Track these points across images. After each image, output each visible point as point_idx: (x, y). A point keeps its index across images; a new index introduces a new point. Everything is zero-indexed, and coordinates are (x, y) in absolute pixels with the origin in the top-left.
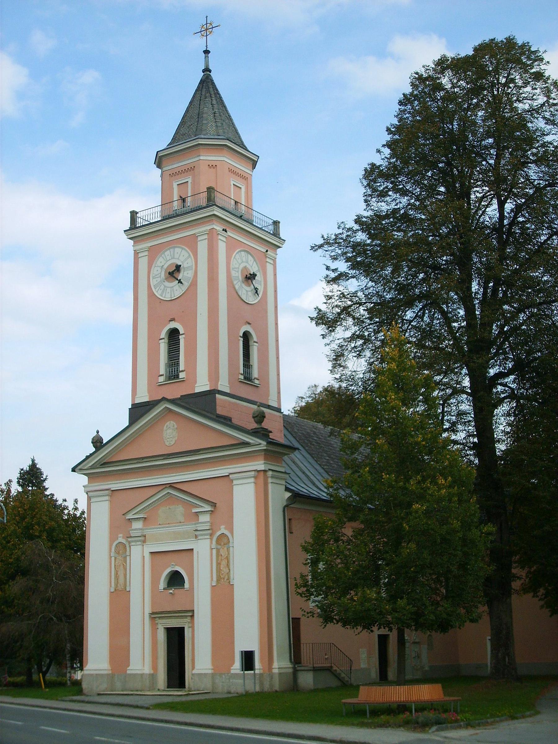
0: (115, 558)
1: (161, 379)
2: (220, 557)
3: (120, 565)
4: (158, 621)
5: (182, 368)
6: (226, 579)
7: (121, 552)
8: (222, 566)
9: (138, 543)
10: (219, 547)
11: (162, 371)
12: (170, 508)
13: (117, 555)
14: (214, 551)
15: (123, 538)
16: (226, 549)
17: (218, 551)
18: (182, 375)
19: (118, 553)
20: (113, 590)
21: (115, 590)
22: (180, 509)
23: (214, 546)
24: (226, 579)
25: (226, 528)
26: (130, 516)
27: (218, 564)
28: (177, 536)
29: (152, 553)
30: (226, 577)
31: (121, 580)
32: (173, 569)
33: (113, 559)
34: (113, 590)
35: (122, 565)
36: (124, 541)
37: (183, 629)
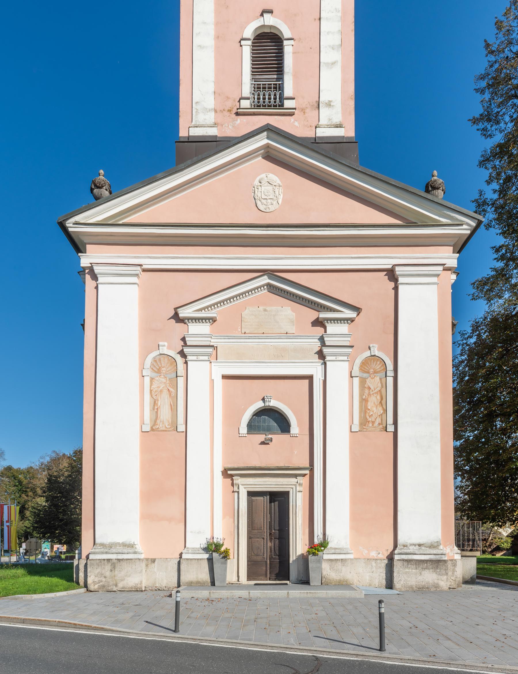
0: (152, 379)
1: (246, 104)
2: (367, 391)
3: (161, 391)
4: (238, 480)
5: (288, 91)
6: (376, 424)
7: (168, 370)
8: (370, 405)
9: (201, 358)
10: (365, 375)
11: (247, 90)
12: (265, 310)
13: (154, 375)
14: (356, 381)
15: (169, 348)
16: (377, 379)
17: (363, 382)
18: (287, 104)
19: (159, 371)
20: (147, 428)
21: (152, 429)
22: (287, 313)
23: (356, 371)
24: (376, 424)
25: (378, 350)
26: (183, 313)
27: (363, 401)
28: (280, 355)
29: (224, 377)
30: (378, 420)
31: (165, 414)
32: (267, 404)
33: (147, 380)
34: (147, 428)
35: (165, 391)
36: (172, 353)
37: (286, 494)
